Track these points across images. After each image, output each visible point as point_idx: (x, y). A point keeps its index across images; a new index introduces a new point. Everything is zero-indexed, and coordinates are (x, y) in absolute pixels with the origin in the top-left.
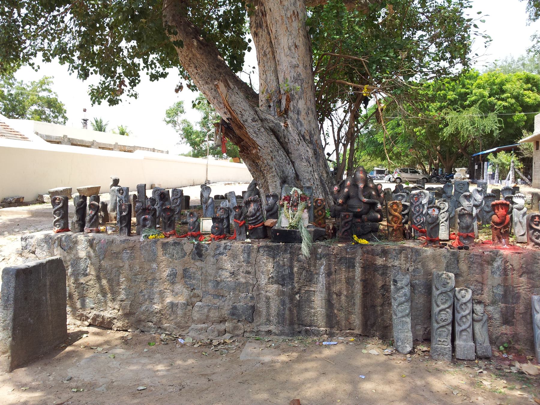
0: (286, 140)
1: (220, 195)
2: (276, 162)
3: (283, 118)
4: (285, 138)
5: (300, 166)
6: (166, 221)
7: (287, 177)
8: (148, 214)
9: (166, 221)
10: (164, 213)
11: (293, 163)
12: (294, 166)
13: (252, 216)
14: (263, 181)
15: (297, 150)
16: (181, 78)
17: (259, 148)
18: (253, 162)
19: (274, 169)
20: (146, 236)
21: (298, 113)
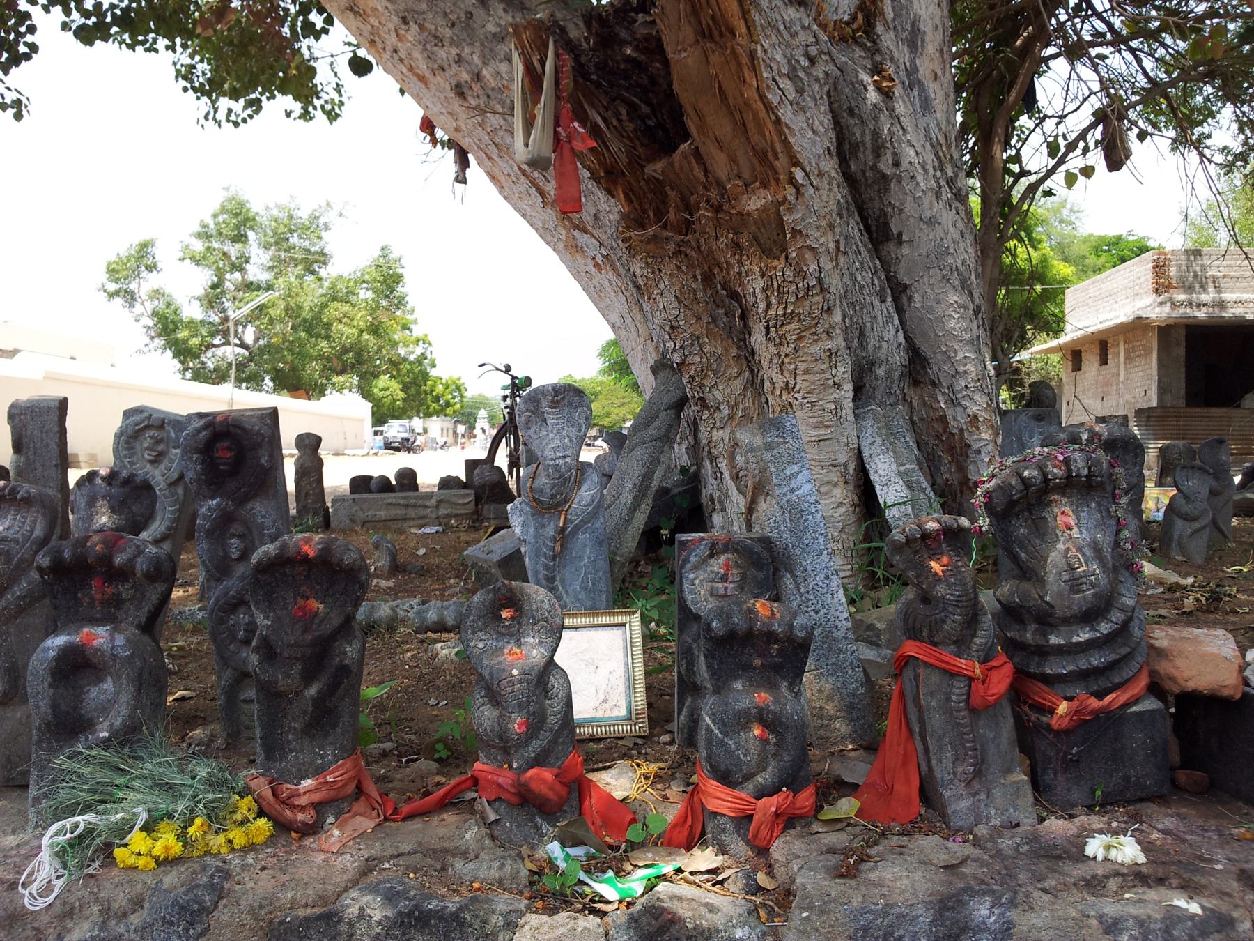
0: (885, 166)
1: (375, 474)
2: (846, 279)
3: (859, 52)
4: (878, 150)
5: (940, 309)
6: (286, 678)
7: (872, 364)
8: (109, 614)
9: (286, 678)
10: (269, 601)
11: (898, 292)
12: (900, 310)
13: (1089, 617)
14: (737, 385)
15: (932, 222)
16: (185, 90)
17: (799, 175)
18: (708, 279)
19: (837, 317)
20: (81, 840)
21: (914, 40)
